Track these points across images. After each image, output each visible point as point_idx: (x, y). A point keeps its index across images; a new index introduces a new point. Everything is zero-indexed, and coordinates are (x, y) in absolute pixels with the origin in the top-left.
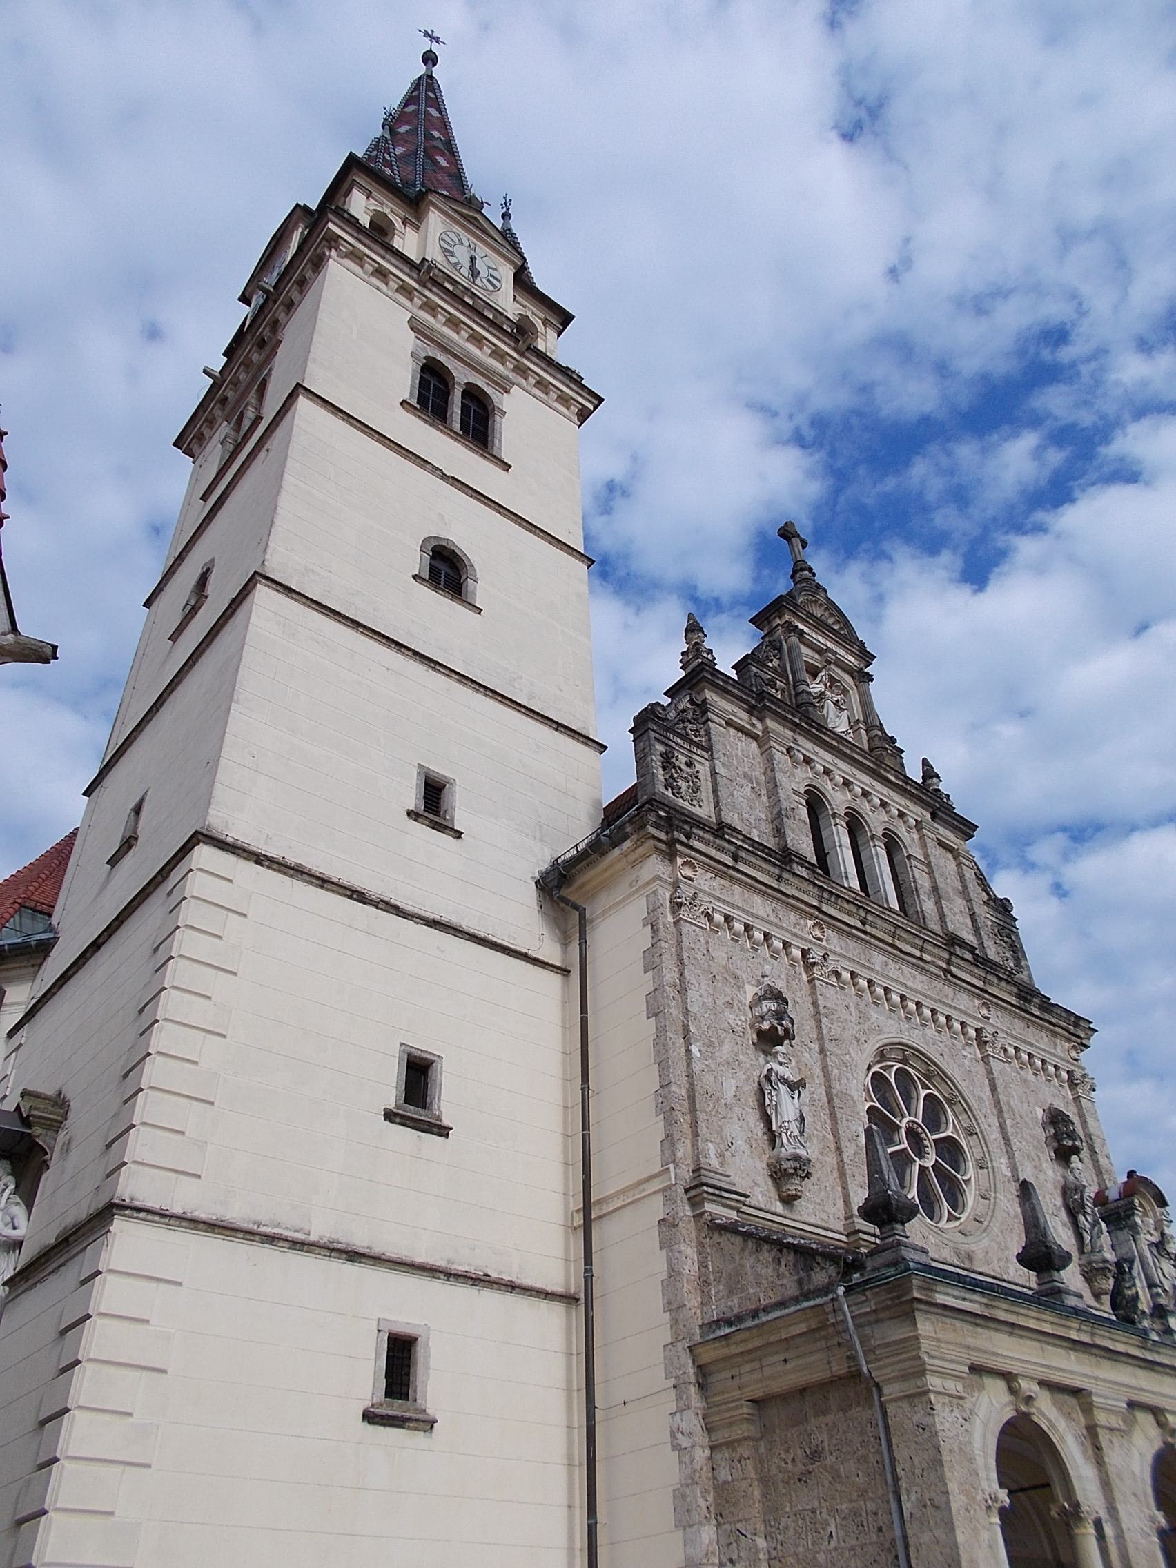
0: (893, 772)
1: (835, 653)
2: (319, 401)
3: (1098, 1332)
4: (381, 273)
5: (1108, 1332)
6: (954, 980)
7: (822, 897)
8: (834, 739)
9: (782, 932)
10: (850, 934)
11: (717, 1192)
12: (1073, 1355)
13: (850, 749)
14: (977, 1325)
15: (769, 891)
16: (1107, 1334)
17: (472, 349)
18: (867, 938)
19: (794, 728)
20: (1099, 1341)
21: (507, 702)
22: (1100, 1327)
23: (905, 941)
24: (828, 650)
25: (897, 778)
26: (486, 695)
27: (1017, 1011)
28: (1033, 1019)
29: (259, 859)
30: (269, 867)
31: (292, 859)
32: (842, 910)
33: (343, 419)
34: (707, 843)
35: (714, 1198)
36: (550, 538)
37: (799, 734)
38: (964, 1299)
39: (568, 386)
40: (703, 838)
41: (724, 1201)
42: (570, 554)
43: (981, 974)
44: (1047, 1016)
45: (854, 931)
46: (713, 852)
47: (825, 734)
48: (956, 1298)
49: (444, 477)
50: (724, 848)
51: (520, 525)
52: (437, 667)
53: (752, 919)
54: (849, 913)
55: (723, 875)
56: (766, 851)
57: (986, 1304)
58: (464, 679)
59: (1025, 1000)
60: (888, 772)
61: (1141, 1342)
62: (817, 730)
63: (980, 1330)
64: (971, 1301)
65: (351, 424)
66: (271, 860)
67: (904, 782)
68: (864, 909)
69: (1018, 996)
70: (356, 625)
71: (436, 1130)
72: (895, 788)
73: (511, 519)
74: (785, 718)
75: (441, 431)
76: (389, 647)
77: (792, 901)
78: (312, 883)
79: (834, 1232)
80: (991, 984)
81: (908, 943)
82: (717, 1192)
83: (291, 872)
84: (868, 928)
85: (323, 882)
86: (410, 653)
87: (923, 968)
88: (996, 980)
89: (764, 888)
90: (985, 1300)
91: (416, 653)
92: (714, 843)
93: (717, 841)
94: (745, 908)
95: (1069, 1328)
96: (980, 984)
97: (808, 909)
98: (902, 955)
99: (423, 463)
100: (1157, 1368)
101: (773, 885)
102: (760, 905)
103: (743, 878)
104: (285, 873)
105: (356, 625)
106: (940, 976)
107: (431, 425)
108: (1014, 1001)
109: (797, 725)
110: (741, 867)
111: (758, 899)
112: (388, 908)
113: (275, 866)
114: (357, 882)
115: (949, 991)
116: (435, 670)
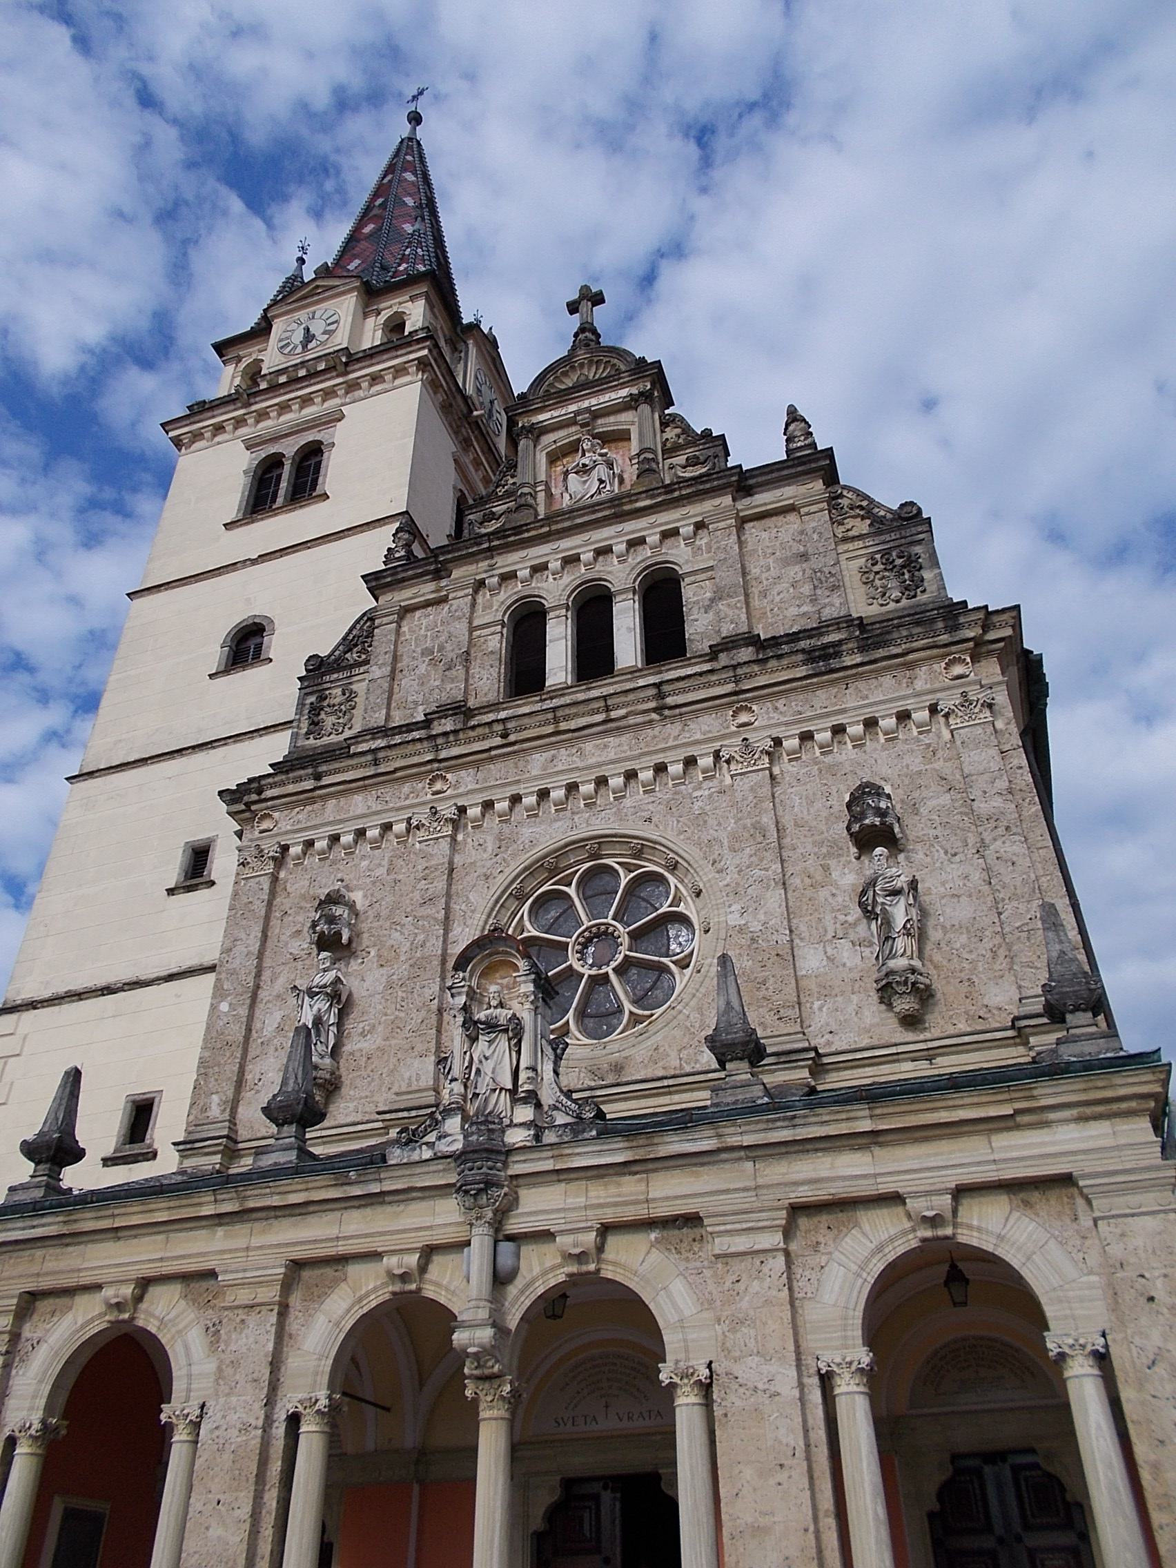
0: (644, 495)
1: (588, 410)
2: (146, 593)
3: (249, 1193)
4: (219, 429)
5: (267, 1187)
6: (677, 711)
7: (437, 745)
8: (542, 526)
9: (384, 815)
10: (492, 758)
11: (188, 1146)
12: (220, 1232)
13: (569, 519)
14: (67, 1245)
15: (367, 782)
16: (268, 1190)
17: (310, 411)
18: (516, 748)
19: (488, 554)
20: (251, 1204)
21: (280, 727)
22: (251, 1187)
23: (576, 715)
24: (577, 413)
25: (652, 497)
26: (261, 736)
27: (815, 680)
28: (854, 671)
29: (33, 1005)
30: (43, 1007)
31: (62, 989)
32: (469, 741)
33: (166, 589)
34: (282, 784)
35: (190, 1152)
36: (359, 529)
37: (499, 554)
38: (34, 1227)
39: (397, 357)
40: (275, 783)
41: (201, 1151)
42: (384, 525)
43: (724, 676)
44: (881, 653)
45: (493, 753)
46: (291, 788)
47: (528, 531)
48: (24, 1229)
49: (254, 562)
50: (301, 777)
51: (330, 541)
52: (214, 745)
53: (341, 826)
54: (484, 738)
55: (312, 801)
56: (404, 729)
57: (65, 1222)
58: (237, 737)
59: (826, 657)
60: (636, 501)
61: (336, 1179)
62: (515, 535)
63: (70, 1249)
64: (43, 1225)
65: (174, 587)
66: (42, 1002)
67: (666, 493)
68: (497, 721)
69: (805, 663)
70: (143, 761)
71: (140, 1158)
72: (659, 509)
73: (320, 544)
74: (473, 554)
75: (262, 519)
76: (174, 758)
77: (399, 774)
78: (73, 1001)
79: (363, 1123)
80: (751, 676)
81: (583, 715)
82: (188, 1146)
83: (56, 1001)
84: (512, 738)
85: (79, 996)
86: (190, 751)
87: (618, 728)
88: (756, 668)
89: (361, 783)
90: (61, 1219)
91: (193, 747)
92: (288, 779)
93: (291, 775)
94: (338, 818)
95: (200, 1204)
96: (730, 687)
97: (423, 769)
98: (576, 734)
99: (233, 567)
100: (387, 1199)
101: (368, 774)
102: (359, 803)
103: (332, 789)
104: (54, 1005)
105: (143, 761)
106: (651, 721)
107: (253, 522)
108: (801, 671)
109: (489, 549)
110: (325, 781)
111: (358, 798)
112: (132, 986)
113: (45, 1004)
114: (101, 982)
115: (678, 726)
116: (214, 748)
